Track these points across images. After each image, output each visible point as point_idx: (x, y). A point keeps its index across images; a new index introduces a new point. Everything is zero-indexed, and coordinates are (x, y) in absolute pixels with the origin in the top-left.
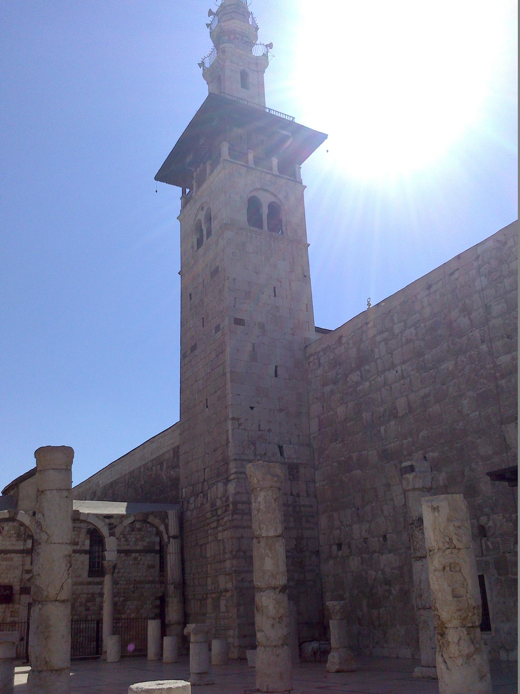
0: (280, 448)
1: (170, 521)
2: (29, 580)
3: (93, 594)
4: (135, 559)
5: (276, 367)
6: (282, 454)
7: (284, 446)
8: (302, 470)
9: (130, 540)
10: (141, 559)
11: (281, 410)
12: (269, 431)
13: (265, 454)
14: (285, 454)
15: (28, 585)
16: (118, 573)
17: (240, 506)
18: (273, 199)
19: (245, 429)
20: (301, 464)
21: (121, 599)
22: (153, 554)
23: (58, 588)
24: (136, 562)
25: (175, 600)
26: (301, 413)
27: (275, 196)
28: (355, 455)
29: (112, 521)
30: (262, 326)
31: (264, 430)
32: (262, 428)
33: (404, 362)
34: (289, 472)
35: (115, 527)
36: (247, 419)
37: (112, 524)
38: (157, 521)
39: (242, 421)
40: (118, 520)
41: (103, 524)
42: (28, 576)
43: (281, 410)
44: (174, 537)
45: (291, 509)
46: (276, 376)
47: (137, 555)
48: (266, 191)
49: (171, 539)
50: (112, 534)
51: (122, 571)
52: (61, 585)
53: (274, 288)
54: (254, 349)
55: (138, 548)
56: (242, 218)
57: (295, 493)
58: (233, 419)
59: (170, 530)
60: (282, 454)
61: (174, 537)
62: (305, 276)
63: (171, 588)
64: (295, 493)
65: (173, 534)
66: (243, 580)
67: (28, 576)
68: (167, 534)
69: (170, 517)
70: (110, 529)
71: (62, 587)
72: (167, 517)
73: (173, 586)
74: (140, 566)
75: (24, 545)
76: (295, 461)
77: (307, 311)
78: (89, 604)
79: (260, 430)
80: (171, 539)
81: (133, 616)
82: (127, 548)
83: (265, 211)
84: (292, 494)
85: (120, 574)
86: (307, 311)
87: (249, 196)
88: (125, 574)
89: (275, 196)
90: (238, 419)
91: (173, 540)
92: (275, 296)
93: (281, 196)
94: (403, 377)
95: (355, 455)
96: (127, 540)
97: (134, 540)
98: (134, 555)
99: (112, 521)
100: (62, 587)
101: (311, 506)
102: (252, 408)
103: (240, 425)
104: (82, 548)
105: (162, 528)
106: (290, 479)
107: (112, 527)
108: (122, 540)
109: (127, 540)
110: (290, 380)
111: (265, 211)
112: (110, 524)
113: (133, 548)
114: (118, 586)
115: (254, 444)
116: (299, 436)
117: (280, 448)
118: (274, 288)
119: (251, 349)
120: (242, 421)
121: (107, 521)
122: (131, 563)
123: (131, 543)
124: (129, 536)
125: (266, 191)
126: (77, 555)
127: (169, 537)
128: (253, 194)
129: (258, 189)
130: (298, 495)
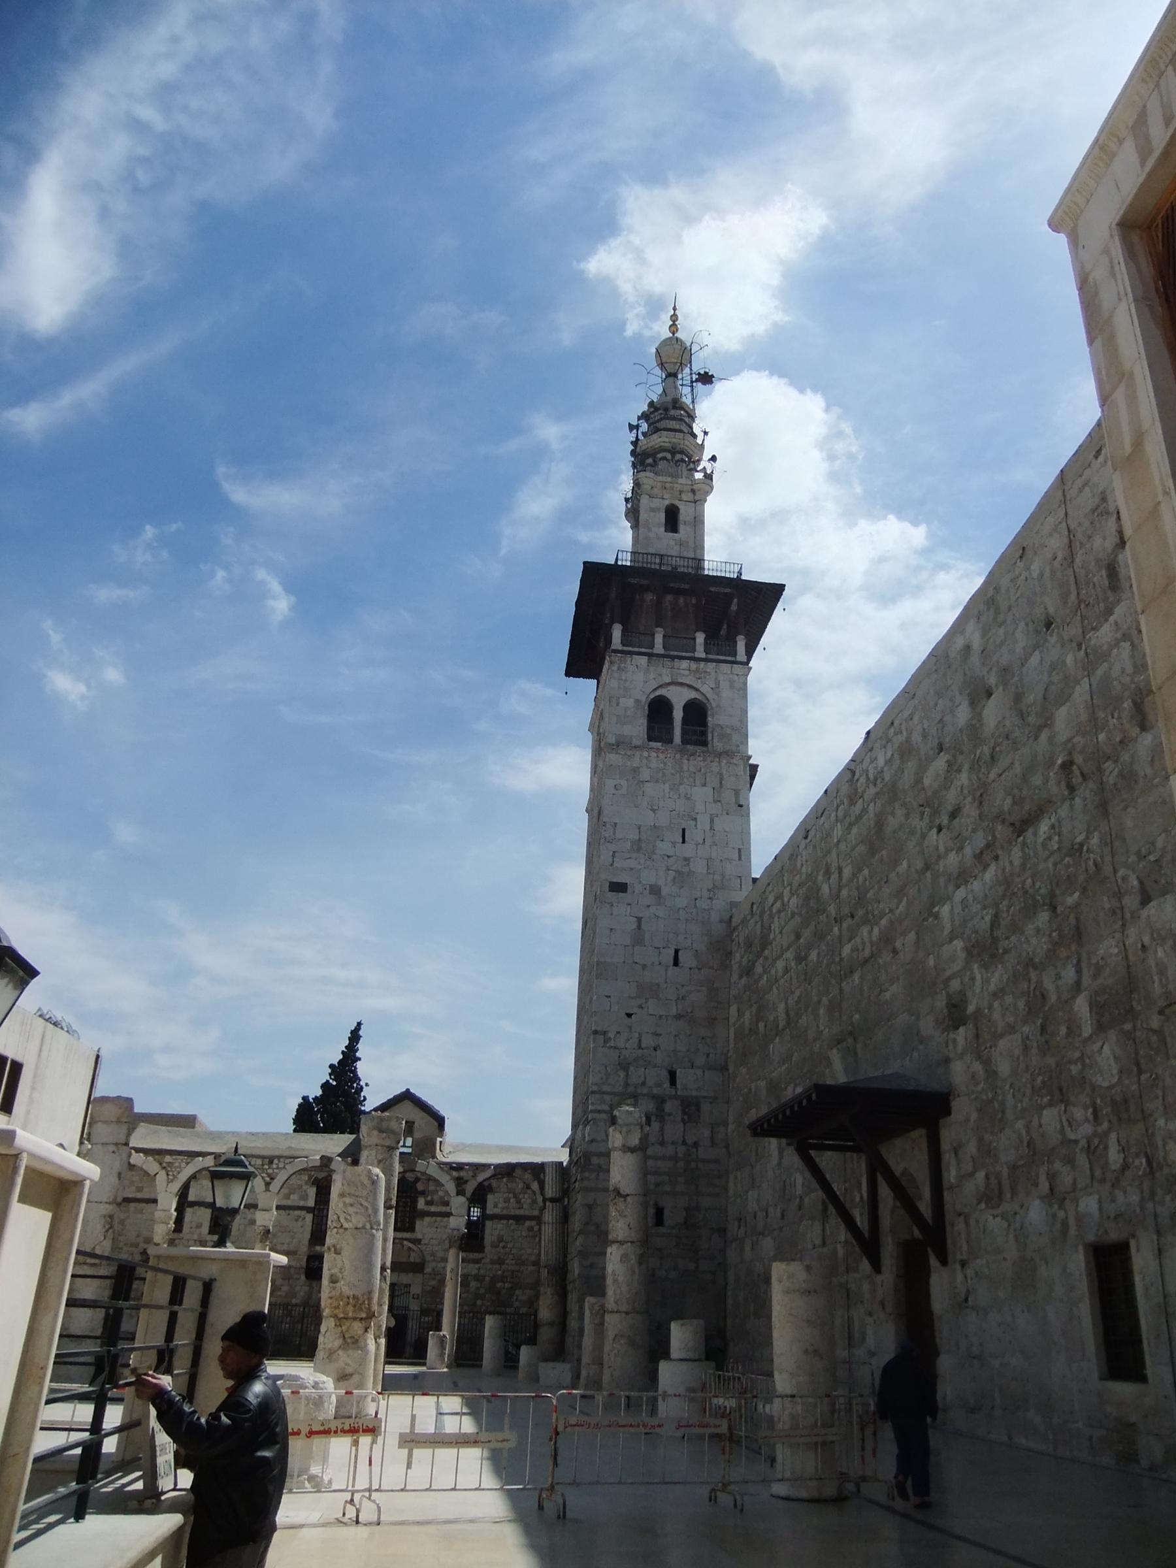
0: (672, 1075)
4: (530, 1229)
5: (677, 952)
6: (673, 1082)
8: (705, 1107)
11: (678, 1017)
13: (644, 1083)
14: (678, 1086)
17: (595, 1160)
18: (693, 695)
19: (615, 1048)
20: (705, 1097)
21: (507, 1285)
25: (549, 1291)
26: (715, 1019)
27: (696, 690)
28: (753, 1086)
29: (462, 1174)
30: (655, 890)
31: (647, 1048)
32: (643, 1045)
33: (788, 948)
34: (684, 1113)
35: (466, 1182)
38: (528, 1176)
39: (611, 1035)
44: (552, 1200)
45: (681, 1164)
46: (676, 963)
48: (682, 684)
49: (548, 1203)
53: (684, 830)
54: (639, 927)
56: (638, 728)
57: (690, 1142)
58: (595, 1032)
60: (673, 1082)
62: (741, 806)
63: (544, 1273)
64: (690, 1142)
66: (592, 1266)
76: (694, 1093)
77: (740, 859)
79: (640, 1047)
80: (548, 1203)
81: (523, 1310)
83: (678, 715)
84: (684, 1143)
86: (740, 859)
87: (652, 696)
89: (696, 690)
90: (605, 1033)
92: (684, 842)
93: (705, 689)
94: (786, 970)
95: (753, 1086)
96: (518, 1201)
97: (529, 1201)
98: (528, 1223)
99: (462, 1174)
101: (717, 1161)
102: (629, 1015)
103: (606, 1041)
106: (683, 1120)
107: (460, 1183)
109: (518, 1201)
110: (700, 969)
111: (678, 715)
113: (527, 1213)
115: (626, 1070)
116: (708, 1055)
117: (672, 1075)
118: (684, 830)
119: (635, 926)
121: (455, 1174)
122: (524, 1234)
123: (525, 1206)
125: (682, 684)
127: (545, 1200)
128: (658, 693)
129: (669, 684)
130: (696, 1145)
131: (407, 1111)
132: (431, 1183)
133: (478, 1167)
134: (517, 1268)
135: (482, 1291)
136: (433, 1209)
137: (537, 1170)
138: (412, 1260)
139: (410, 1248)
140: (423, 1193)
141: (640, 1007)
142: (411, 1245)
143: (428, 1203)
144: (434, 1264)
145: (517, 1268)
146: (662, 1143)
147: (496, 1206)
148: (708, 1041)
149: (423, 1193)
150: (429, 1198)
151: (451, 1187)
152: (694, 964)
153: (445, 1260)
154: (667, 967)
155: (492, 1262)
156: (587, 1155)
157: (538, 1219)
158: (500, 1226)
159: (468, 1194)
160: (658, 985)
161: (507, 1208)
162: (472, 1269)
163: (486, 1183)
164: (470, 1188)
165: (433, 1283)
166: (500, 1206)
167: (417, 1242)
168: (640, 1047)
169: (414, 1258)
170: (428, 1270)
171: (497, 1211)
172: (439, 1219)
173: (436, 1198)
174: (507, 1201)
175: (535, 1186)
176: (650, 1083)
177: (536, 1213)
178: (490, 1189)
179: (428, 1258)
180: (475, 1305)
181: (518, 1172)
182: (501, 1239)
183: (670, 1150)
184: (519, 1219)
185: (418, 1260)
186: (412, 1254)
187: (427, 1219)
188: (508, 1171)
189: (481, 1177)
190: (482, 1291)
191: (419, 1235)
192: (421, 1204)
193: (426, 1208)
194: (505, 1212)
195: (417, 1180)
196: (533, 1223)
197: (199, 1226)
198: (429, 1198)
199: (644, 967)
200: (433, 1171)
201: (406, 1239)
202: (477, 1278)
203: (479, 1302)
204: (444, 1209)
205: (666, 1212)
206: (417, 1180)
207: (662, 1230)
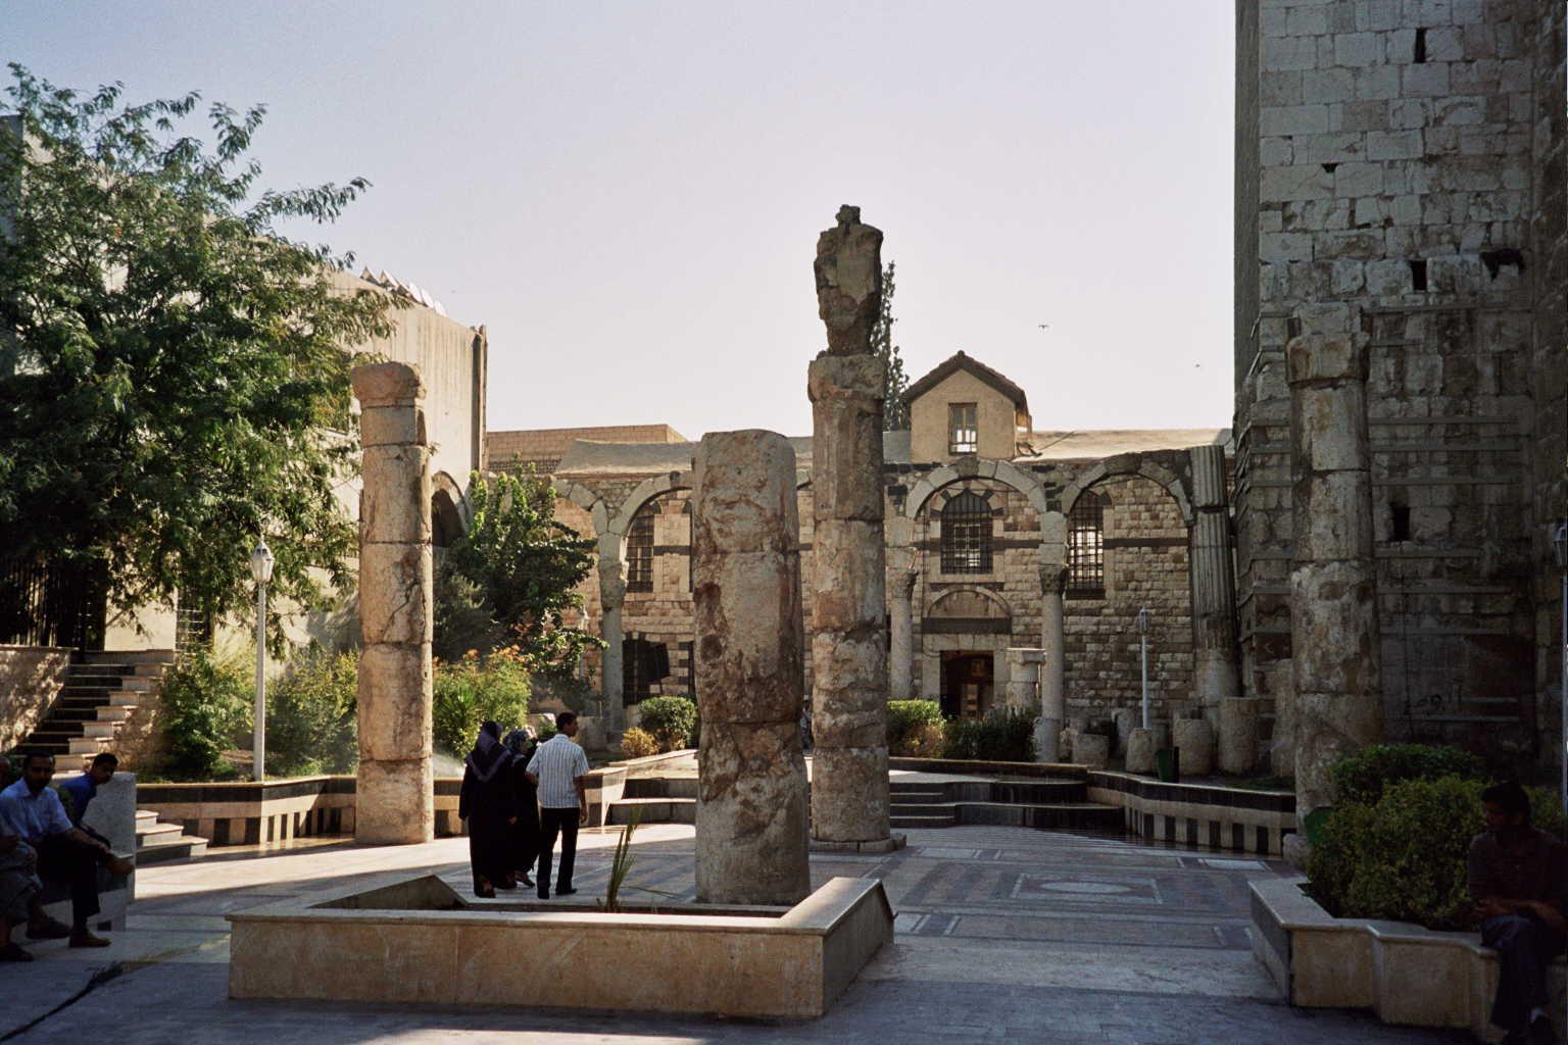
0: (1418, 271)
1: (1195, 471)
2: (939, 603)
3: (1079, 635)
4: (1177, 559)
5: (1421, 33)
6: (1420, 283)
7: (1429, 260)
9: (1162, 515)
11: (1429, 160)
12: (1388, 222)
13: (1363, 289)
15: (939, 614)
16: (1135, 590)
19: (1305, 231)
23: (384, 621)
24: (1179, 566)
29: (1053, 476)
31: (1367, 225)
35: (1061, 489)
36: (1310, 202)
37: (1054, 484)
38: (1162, 472)
39: (1295, 208)
40: (1067, 475)
41: (1030, 483)
42: (936, 596)
43: (1429, 160)
44: (1207, 509)
46: (1420, 55)
50: (1052, 506)
51: (1147, 585)
52: (389, 615)
59: (1197, 493)
61: (1207, 509)
65: (1203, 503)
67: (936, 596)
68: (1189, 501)
69: (1195, 463)
70: (1048, 495)
71: (392, 617)
72: (1190, 463)
73: (1205, 621)
75: (925, 532)
82: (1155, 534)
85: (1143, 593)
88: (1152, 594)
90: (1285, 205)
91: (1205, 516)
96: (1155, 517)
98: (1173, 550)
99: (1053, 476)
100: (392, 617)
102: (1330, 168)
103: (1287, 220)
107: (1052, 492)
108: (1145, 515)
109: (1155, 517)
112: (1047, 485)
113: (1172, 534)
115: (1326, 268)
116: (1489, 225)
117: (1418, 271)
120: (1295, 208)
121: (1041, 476)
122: (1169, 566)
124: (1159, 507)
127: (1194, 510)
131: (961, 388)
132: (1011, 496)
133: (1078, 466)
134: (1160, 619)
135: (1106, 657)
136: (1018, 536)
137: (1177, 462)
138: (992, 615)
139: (987, 598)
140: (999, 512)
141: (1351, 149)
142: (988, 593)
143: (1008, 528)
144: (1027, 619)
145: (1160, 619)
146: (1403, 395)
147: (1117, 527)
148: (1490, 198)
149: (999, 512)
150: (1010, 520)
151: (1037, 498)
152: (1457, 53)
153: (1039, 612)
154: (1401, 67)
155: (1118, 613)
156: (1250, 427)
157: (1188, 542)
158: (1127, 557)
159: (1066, 507)
160: (1386, 103)
161: (1137, 528)
162: (1086, 624)
163: (1098, 490)
164: (1067, 498)
166: (1124, 525)
167: (999, 586)
168: (1352, 225)
169: (994, 612)
170: (1018, 629)
171: (1118, 534)
172: (1029, 551)
173: (1020, 518)
174: (1136, 516)
175: (1177, 487)
176: (1375, 288)
177: (1184, 533)
178: (1106, 500)
180: (1096, 677)
181: (1146, 467)
182: (1130, 576)
183: (1419, 404)
184: (1157, 544)
185: (1003, 616)
186: (993, 607)
187: (1010, 552)
188: (1131, 466)
189: (1084, 480)
190: (1106, 657)
191: (1000, 578)
192: (998, 529)
194: (1133, 534)
195: (989, 492)
196: (1183, 549)
197: (675, 582)
198: (1010, 520)
199: (1356, 71)
200: (1006, 475)
201: (980, 584)
202: (1098, 637)
203: (1102, 674)
204: (1034, 535)
205: (1415, 517)
206: (989, 492)
207: (1406, 545)
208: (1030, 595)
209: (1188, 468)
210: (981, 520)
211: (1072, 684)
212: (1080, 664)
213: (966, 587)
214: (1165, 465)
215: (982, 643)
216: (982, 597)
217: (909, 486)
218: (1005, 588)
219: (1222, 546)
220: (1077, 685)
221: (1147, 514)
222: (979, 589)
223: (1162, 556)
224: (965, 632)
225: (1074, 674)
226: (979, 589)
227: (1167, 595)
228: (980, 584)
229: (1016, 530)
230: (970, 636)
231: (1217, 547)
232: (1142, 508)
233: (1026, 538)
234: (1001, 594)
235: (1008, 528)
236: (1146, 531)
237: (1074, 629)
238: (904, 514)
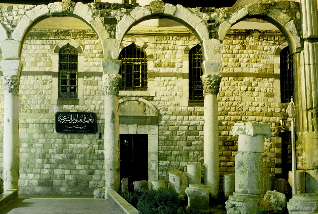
9: (240, 60)
10: (256, 85)
16: (226, 101)
22: (270, 80)
47: (251, 79)
55: (253, 70)
68: (300, 35)
70: (210, 28)
74: (255, 93)
78: (190, 138)
80: (306, 43)
82: (237, 70)
91: (310, 44)
97: (245, 60)
98: (246, 79)
104: (180, 71)
105: (290, 27)
108: (231, 60)
114: (227, 117)
124: (239, 55)
126: (173, 78)
127: (302, 40)
136: (162, 70)
140: (151, 56)
143: (156, 66)
144: (166, 117)
150: (158, 61)
165: (168, 133)
179: (162, 113)
193: (156, 70)
201: (141, 96)
208: (168, 104)
209: (298, 13)
210: (142, 61)
211: (191, 154)
212: (195, 142)
213: (133, 98)
214: (284, 11)
215: (142, 131)
216: (142, 104)
217: (118, 18)
218: (155, 98)
219: (314, 64)
220: (194, 154)
221: (232, 59)
222: (141, 99)
223: (240, 82)
224: (133, 123)
225: (192, 148)
226: (141, 99)
227: (243, 104)
228: (141, 96)
229: (161, 67)
230: (135, 126)
231: (309, 64)
232: (229, 55)
233: (166, 72)
234: (152, 102)
235: (156, 66)
236: (232, 69)
237: (192, 123)
238: (114, 37)
